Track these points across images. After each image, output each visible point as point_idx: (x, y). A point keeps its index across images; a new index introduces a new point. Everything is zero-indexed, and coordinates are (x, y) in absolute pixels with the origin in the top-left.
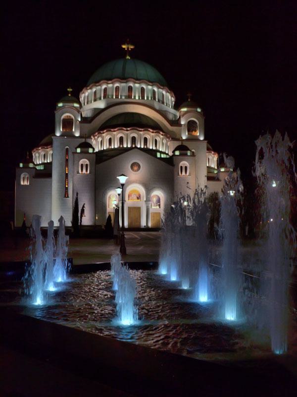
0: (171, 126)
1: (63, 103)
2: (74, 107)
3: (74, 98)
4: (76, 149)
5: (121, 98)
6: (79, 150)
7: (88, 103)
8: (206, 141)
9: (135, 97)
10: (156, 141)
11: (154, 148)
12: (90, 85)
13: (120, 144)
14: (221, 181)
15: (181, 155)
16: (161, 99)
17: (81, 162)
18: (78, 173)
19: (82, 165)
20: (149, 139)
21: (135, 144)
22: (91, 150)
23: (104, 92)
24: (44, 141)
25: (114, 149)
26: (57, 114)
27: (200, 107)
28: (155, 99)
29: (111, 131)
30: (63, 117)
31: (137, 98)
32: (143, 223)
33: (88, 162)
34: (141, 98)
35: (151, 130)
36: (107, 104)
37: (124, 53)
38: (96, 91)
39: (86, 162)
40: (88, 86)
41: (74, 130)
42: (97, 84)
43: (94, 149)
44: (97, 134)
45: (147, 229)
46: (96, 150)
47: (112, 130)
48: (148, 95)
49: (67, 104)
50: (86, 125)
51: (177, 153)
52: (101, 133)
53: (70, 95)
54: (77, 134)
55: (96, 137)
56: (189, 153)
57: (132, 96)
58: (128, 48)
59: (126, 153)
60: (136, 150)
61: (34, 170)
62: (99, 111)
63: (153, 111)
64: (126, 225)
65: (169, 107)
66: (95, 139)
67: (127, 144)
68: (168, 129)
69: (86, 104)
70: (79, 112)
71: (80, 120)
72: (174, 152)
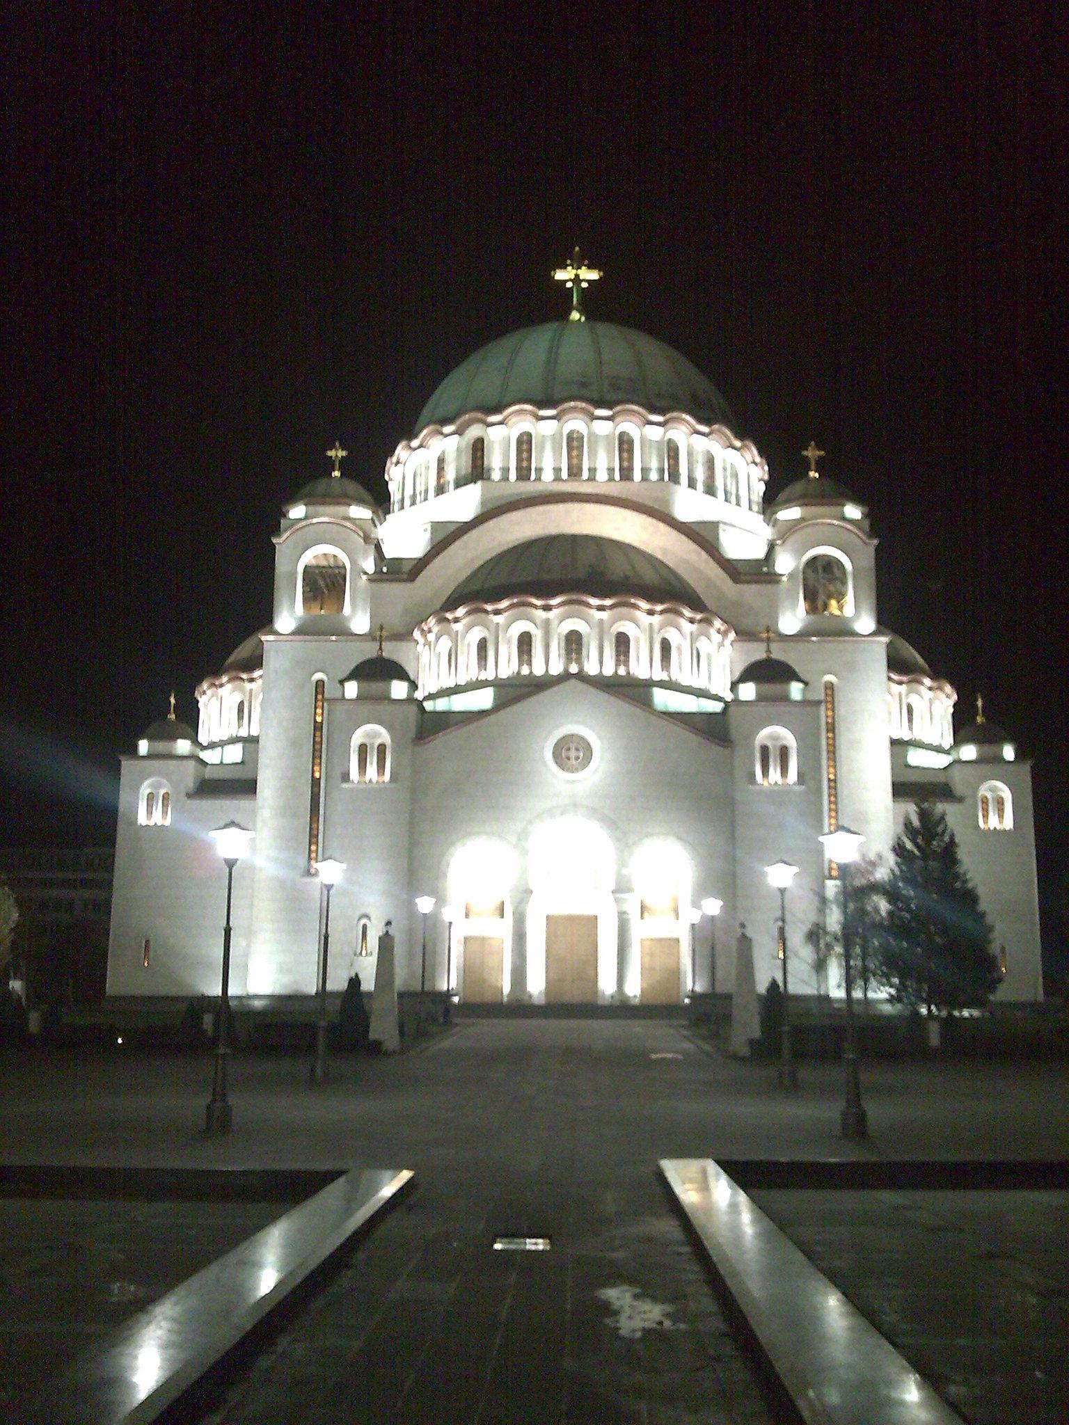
2: (348, 519)
3: (352, 487)
4: (342, 682)
6: (352, 689)
7: (413, 503)
8: (884, 639)
9: (592, 471)
10: (666, 647)
11: (659, 675)
12: (421, 431)
13: (521, 663)
14: (960, 800)
15: (761, 698)
17: (358, 738)
18: (346, 777)
19: (363, 749)
20: (637, 640)
21: (579, 661)
22: (399, 689)
24: (243, 651)
26: (283, 543)
27: (858, 500)
28: (675, 477)
30: (308, 558)
31: (602, 476)
32: (607, 986)
33: (384, 736)
34: (617, 477)
35: (644, 605)
36: (483, 503)
37: (559, 300)
39: (377, 735)
40: (411, 435)
41: (347, 610)
42: (448, 429)
43: (414, 686)
44: (432, 621)
45: (621, 1009)
46: (428, 684)
47: (489, 607)
48: (647, 461)
49: (321, 509)
50: (396, 590)
51: (748, 691)
52: (448, 620)
53: (337, 474)
54: (360, 622)
55: (431, 637)
56: (795, 690)
57: (581, 469)
58: (577, 280)
59: (534, 699)
60: (581, 686)
61: (192, 763)
62: (453, 528)
63: (661, 525)
64: (536, 986)
65: (738, 504)
66: (427, 643)
69: (407, 502)
70: (367, 538)
71: (369, 565)
72: (734, 686)
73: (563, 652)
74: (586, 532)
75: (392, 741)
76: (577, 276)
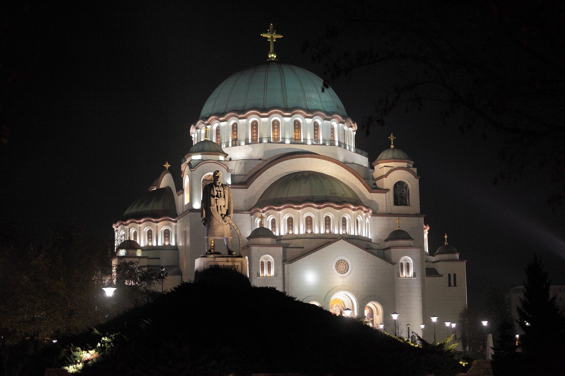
0: (370, 192)
1: (201, 154)
2: (219, 161)
5: (283, 143)
9: (305, 139)
11: (356, 234)
13: (307, 228)
14: (442, 276)
16: (342, 141)
17: (262, 259)
18: (258, 275)
21: (329, 228)
23: (252, 129)
25: (298, 237)
29: (294, 208)
31: (309, 142)
33: (271, 259)
35: (352, 207)
38: (236, 124)
47: (295, 206)
67: (319, 229)
68: (365, 198)
73: (324, 225)
74: (313, 170)
75: (275, 261)
76: (272, 37)
